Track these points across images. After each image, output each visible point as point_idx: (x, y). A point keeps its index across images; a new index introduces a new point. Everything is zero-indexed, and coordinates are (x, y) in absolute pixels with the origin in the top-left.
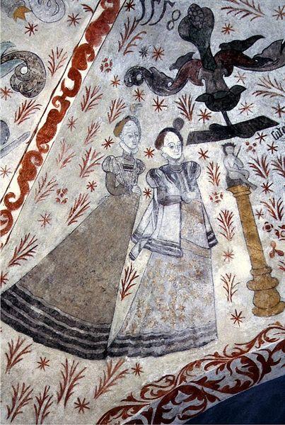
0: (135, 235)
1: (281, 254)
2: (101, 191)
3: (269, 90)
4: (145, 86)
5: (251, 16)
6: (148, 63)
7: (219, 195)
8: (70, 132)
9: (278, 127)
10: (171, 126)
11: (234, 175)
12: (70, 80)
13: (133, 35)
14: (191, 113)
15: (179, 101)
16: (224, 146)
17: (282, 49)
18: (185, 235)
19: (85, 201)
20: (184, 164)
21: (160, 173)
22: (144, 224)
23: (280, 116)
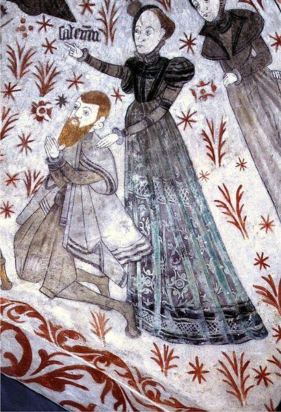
9: (73, 25)
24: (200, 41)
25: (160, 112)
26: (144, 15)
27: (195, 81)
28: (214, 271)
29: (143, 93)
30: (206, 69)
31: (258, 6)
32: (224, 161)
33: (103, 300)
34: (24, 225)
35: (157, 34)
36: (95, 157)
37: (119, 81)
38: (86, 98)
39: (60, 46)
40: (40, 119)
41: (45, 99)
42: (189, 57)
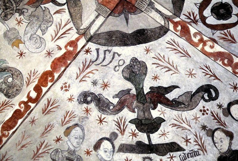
3: (181, 125)
4: (92, 106)
5: (171, 72)
6: (97, 90)
8: (31, 127)
9: (185, 152)
10: (108, 136)
12: (34, 92)
13: (89, 70)
14: (124, 130)
15: (117, 120)
17: (191, 98)
23: (187, 145)
26: (216, 134)
35: (227, 141)
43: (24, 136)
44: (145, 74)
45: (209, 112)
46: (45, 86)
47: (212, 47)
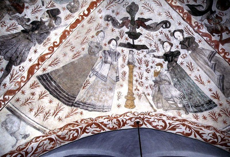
0: (93, 70)
1: (138, 90)
2: (86, 51)
3: (149, 37)
4: (110, 23)
5: (150, 12)
6: (113, 15)
7: (124, 66)
9: (149, 50)
10: (115, 38)
11: (131, 61)
13: (112, 4)
14: (122, 36)
15: (120, 31)
16: (130, 51)
18: (109, 75)
19: (80, 53)
20: (116, 52)
21: (107, 52)
22: (97, 67)
23: (150, 47)
24: (180, 46)
25: (175, 64)
26: (165, 43)
27: (181, 55)
28: (200, 95)
29: (170, 60)
30: (183, 52)
31: (192, 35)
32: (194, 70)
33: (178, 108)
34: (154, 97)
35: (169, 47)
36: (163, 77)
37: (163, 59)
38: (157, 65)
39: (147, 55)
40: (148, 72)
41: (148, 68)
42: (178, 50)
43: (78, 33)
44: (137, 11)
45: (164, 33)
46: (92, 9)
47: (175, 3)
